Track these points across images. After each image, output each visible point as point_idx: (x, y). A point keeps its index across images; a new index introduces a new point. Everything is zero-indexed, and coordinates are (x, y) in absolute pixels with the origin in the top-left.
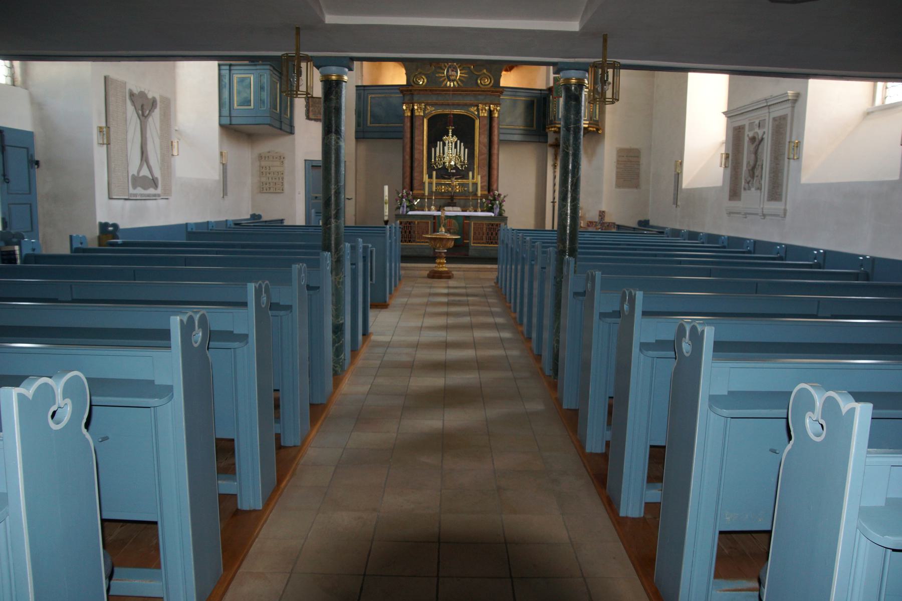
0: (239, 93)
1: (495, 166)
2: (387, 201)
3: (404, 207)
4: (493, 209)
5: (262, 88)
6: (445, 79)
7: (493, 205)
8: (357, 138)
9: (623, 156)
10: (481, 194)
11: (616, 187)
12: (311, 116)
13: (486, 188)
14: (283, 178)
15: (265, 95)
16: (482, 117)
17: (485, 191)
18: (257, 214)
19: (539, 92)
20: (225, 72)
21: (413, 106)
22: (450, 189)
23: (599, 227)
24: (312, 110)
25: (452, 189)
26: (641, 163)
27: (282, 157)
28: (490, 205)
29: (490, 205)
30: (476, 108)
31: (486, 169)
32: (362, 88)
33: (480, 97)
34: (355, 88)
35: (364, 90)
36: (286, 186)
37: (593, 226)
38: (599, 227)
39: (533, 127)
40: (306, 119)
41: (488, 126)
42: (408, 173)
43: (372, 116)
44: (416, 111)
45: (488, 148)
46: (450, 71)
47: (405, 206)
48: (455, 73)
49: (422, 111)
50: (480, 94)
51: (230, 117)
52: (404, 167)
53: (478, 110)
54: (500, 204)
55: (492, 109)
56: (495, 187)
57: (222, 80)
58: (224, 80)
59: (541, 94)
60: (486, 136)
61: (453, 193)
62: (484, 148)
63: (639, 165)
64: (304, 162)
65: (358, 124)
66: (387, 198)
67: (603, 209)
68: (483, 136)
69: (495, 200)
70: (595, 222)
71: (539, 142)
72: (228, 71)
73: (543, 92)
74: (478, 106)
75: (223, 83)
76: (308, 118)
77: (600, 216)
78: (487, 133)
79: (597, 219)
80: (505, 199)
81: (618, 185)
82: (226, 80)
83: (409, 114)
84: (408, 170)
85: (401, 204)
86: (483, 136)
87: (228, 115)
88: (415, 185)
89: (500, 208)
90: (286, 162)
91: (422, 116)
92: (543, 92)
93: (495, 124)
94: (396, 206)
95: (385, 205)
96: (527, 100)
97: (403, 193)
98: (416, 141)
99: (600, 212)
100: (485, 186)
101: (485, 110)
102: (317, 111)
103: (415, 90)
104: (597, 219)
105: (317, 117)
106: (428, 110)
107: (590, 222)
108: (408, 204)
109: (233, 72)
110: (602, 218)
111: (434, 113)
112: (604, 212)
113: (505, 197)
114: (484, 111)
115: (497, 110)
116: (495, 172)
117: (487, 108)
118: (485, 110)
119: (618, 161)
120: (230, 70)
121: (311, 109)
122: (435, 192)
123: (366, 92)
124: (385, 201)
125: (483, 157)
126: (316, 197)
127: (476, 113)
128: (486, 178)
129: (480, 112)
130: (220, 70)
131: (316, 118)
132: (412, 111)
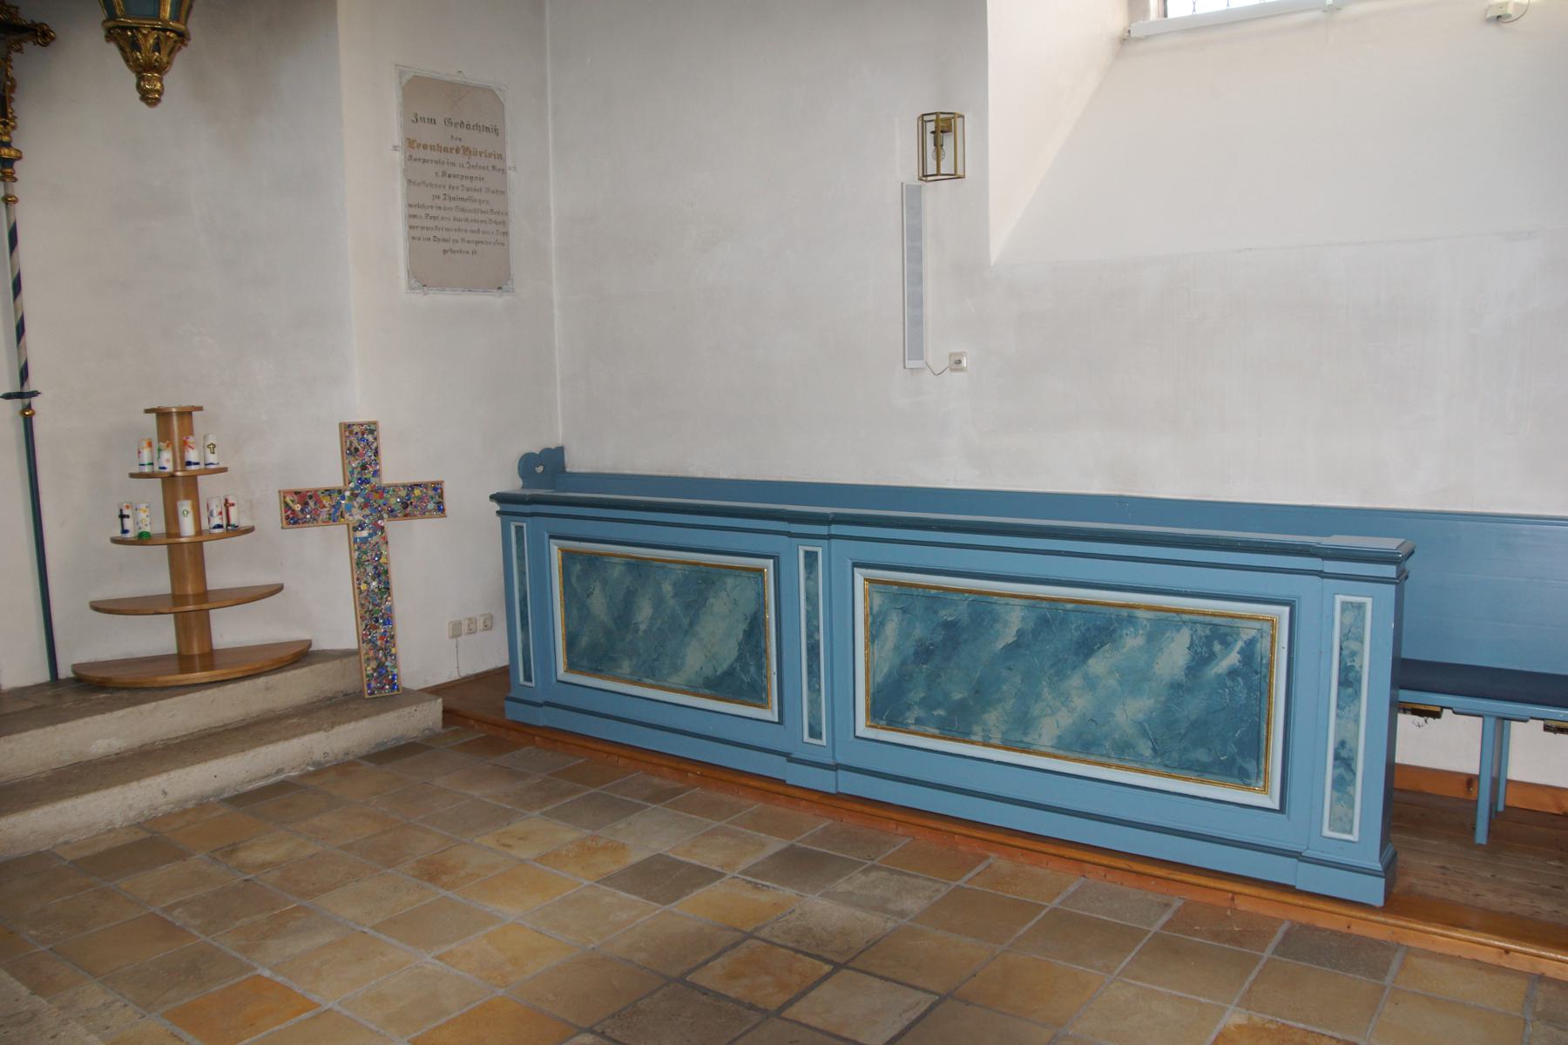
9: (433, 121)
11: (411, 288)
23: (357, 515)
26: (509, 163)
37: (324, 516)
38: (357, 515)
63: (503, 171)
67: (360, 415)
70: (329, 492)
77: (351, 452)
79: (328, 472)
81: (421, 279)
99: (347, 428)
104: (328, 472)
107: (303, 497)
110: (364, 467)
112: (371, 428)
119: (411, 143)
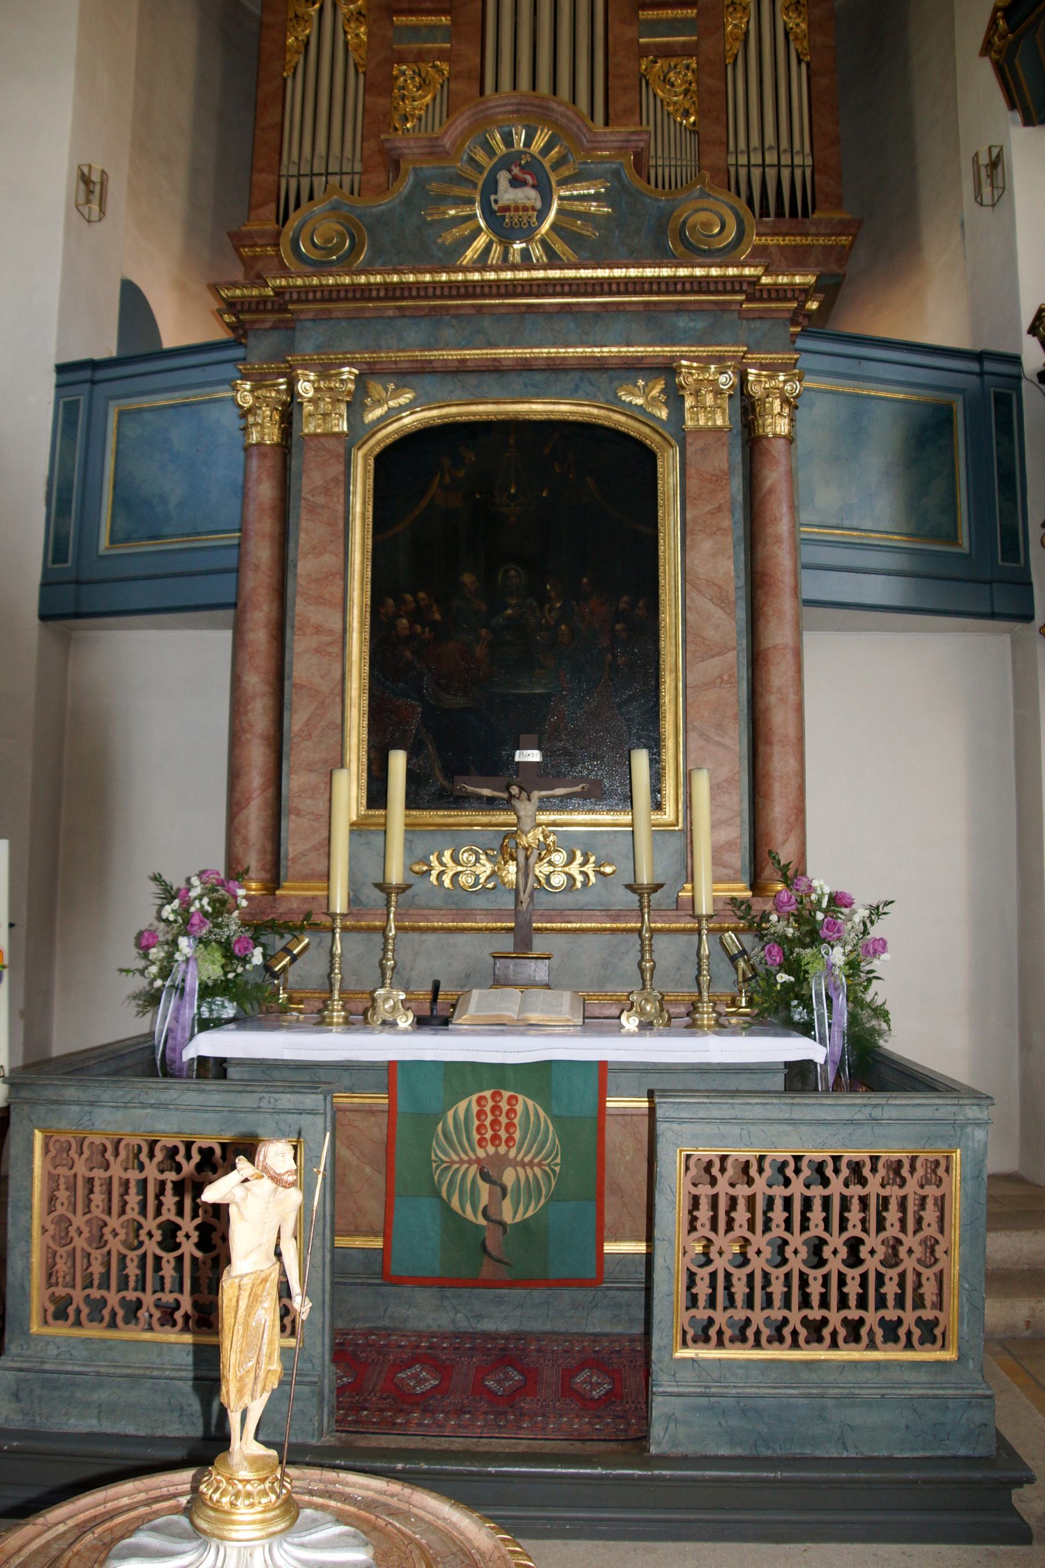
1: (779, 719)
3: (181, 991)
4: (806, 1002)
10: (715, 900)
13: (739, 859)
16: (699, 431)
17: (734, 881)
19: (974, 366)
21: (292, 384)
22: (512, 867)
25: (525, 871)
28: (783, 978)
29: (783, 978)
30: (660, 386)
31: (736, 739)
32: (86, 374)
34: (52, 378)
39: (952, 538)
41: (736, 484)
42: (256, 780)
44: (309, 408)
45: (742, 614)
47: (193, 984)
48: (533, 194)
49: (343, 408)
50: (680, 308)
53: (674, 397)
54: (853, 965)
55: (756, 390)
59: (981, 374)
60: (728, 541)
61: (524, 897)
62: (718, 613)
71: (993, 616)
73: (989, 366)
74: (668, 369)
78: (733, 523)
80: (876, 931)
83: (271, 435)
84: (257, 755)
85: (165, 973)
86: (706, 545)
89: (855, 1000)
91: (338, 435)
92: (989, 366)
93: (774, 476)
94: (139, 984)
96: (914, 403)
98: (301, 582)
100: (729, 846)
101: (718, 393)
108: (213, 971)
111: (409, 421)
113: (876, 912)
114: (709, 400)
115: (785, 401)
117: (726, 380)
118: (718, 393)
122: (403, 889)
123: (101, 390)
125: (711, 667)
127: (663, 414)
128: (739, 800)
129: (689, 402)
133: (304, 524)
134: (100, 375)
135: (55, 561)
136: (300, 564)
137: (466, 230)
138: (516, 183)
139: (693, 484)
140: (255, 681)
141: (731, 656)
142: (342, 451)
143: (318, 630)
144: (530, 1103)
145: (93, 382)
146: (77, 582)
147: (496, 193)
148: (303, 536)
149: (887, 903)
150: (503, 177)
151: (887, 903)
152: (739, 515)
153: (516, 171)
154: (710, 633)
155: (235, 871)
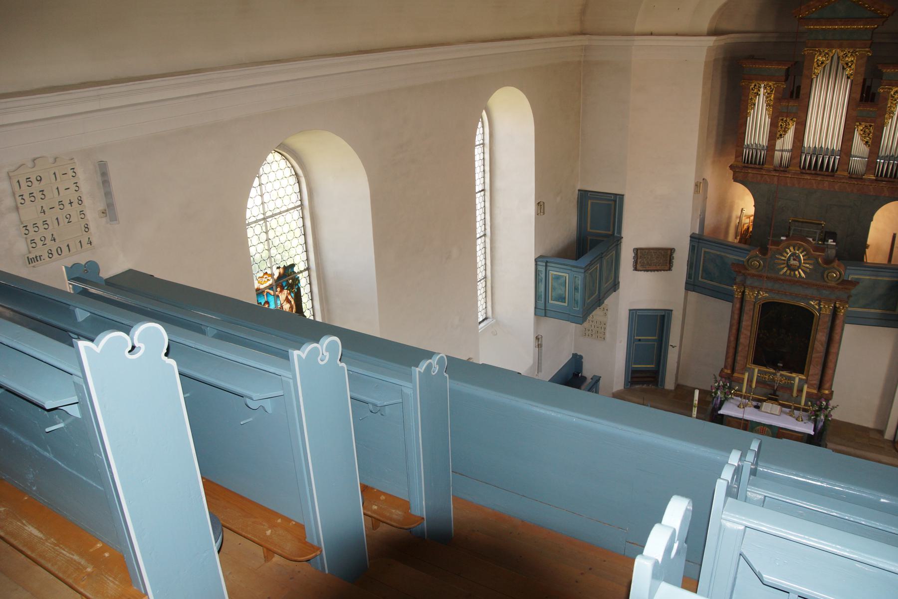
0: (554, 289)
1: (830, 365)
2: (697, 405)
5: (576, 289)
6: (784, 267)
7: (817, 416)
8: (687, 289)
12: (639, 267)
14: (605, 329)
15: (579, 296)
17: (815, 389)
18: (579, 354)
20: (542, 269)
24: (640, 262)
27: (605, 309)
32: (697, 240)
33: (824, 291)
35: (699, 242)
36: (608, 335)
40: (634, 270)
41: (829, 324)
42: (731, 354)
43: (705, 270)
46: (792, 260)
51: (545, 310)
52: (728, 347)
55: (837, 305)
56: (827, 385)
57: (539, 274)
58: (540, 274)
64: (628, 311)
65: (689, 276)
66: (697, 402)
68: (821, 334)
69: (821, 409)
72: (544, 268)
74: (820, 301)
75: (540, 278)
76: (636, 269)
82: (543, 276)
84: (732, 351)
86: (821, 334)
87: (543, 308)
88: (736, 369)
90: (609, 313)
95: (694, 408)
97: (719, 384)
98: (743, 326)
102: (645, 262)
103: (749, 274)
105: (645, 268)
106: (761, 295)
109: (549, 268)
116: (829, 372)
120: (546, 266)
121: (639, 261)
124: (694, 405)
126: (640, 340)
127: (817, 307)
130: (536, 265)
131: (644, 269)
132: (743, 292)
133: (745, 315)
134: (700, 241)
135: (689, 278)
136: (743, 323)
137: (783, 266)
138: (794, 260)
139: (820, 323)
140: (732, 339)
141: (822, 354)
142: (753, 303)
143: (745, 334)
144: (769, 430)
145: (699, 242)
146: (694, 285)
147: (790, 261)
148: (744, 318)
149: (838, 406)
150: (792, 257)
151: (838, 406)
152: (829, 329)
153: (795, 257)
154: (818, 349)
155: (726, 367)
